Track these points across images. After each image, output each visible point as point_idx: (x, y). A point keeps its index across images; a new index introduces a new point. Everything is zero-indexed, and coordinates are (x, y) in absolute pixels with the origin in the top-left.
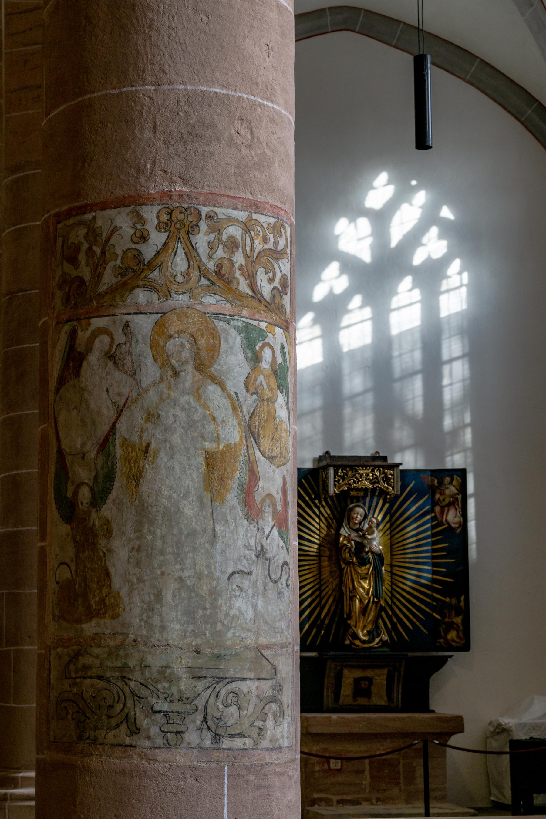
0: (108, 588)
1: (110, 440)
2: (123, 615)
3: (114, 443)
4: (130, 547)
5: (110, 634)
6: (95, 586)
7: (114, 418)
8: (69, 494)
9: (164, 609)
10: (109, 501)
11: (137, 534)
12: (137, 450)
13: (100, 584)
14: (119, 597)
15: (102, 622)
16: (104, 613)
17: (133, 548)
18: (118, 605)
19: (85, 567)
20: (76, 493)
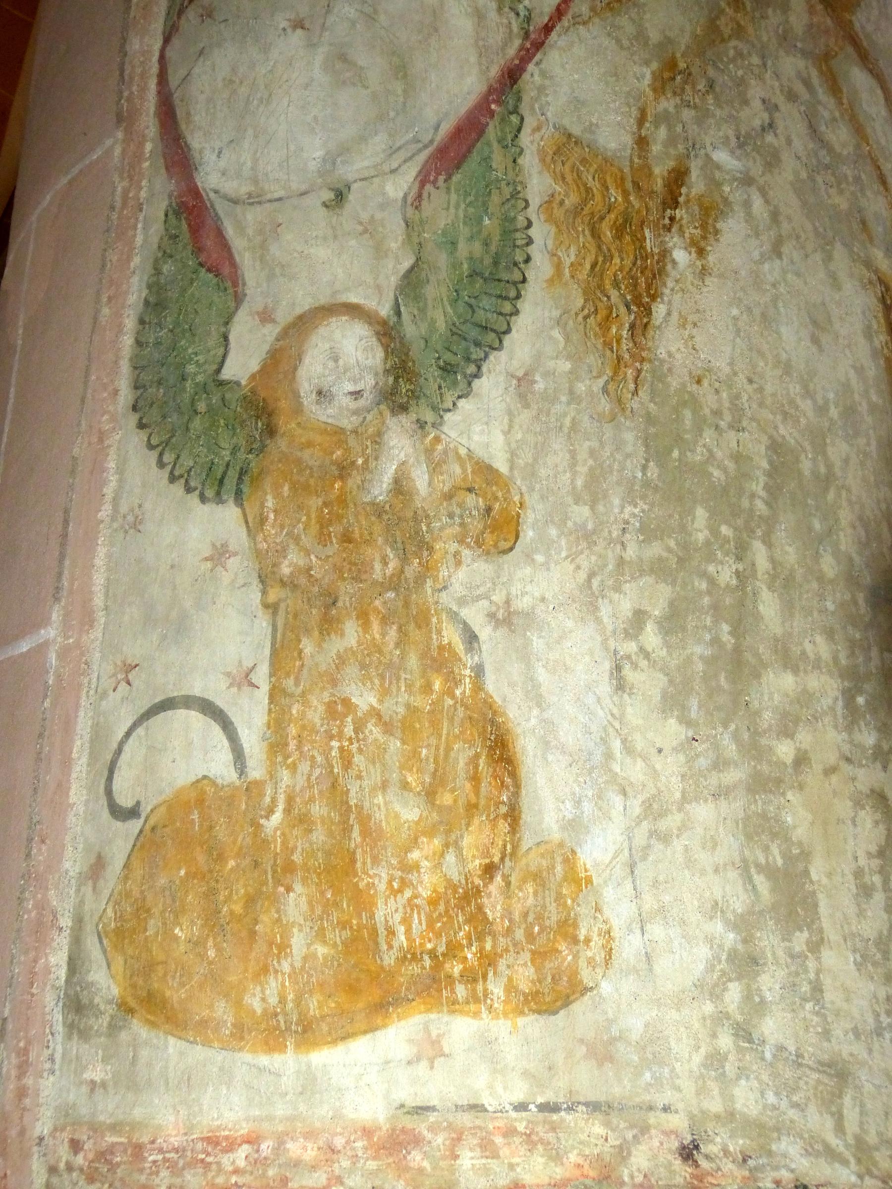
0: (503, 826)
1: (492, 131)
2: (606, 987)
3: (511, 143)
4: (626, 606)
5: (521, 1107)
6: (410, 812)
7: (512, 51)
8: (242, 365)
9: (829, 957)
10: (492, 385)
11: (656, 549)
12: (629, 185)
13: (446, 799)
14: (578, 880)
15: (460, 1029)
16: (471, 977)
17: (639, 617)
18: (567, 929)
19: (341, 708)
20: (281, 361)
